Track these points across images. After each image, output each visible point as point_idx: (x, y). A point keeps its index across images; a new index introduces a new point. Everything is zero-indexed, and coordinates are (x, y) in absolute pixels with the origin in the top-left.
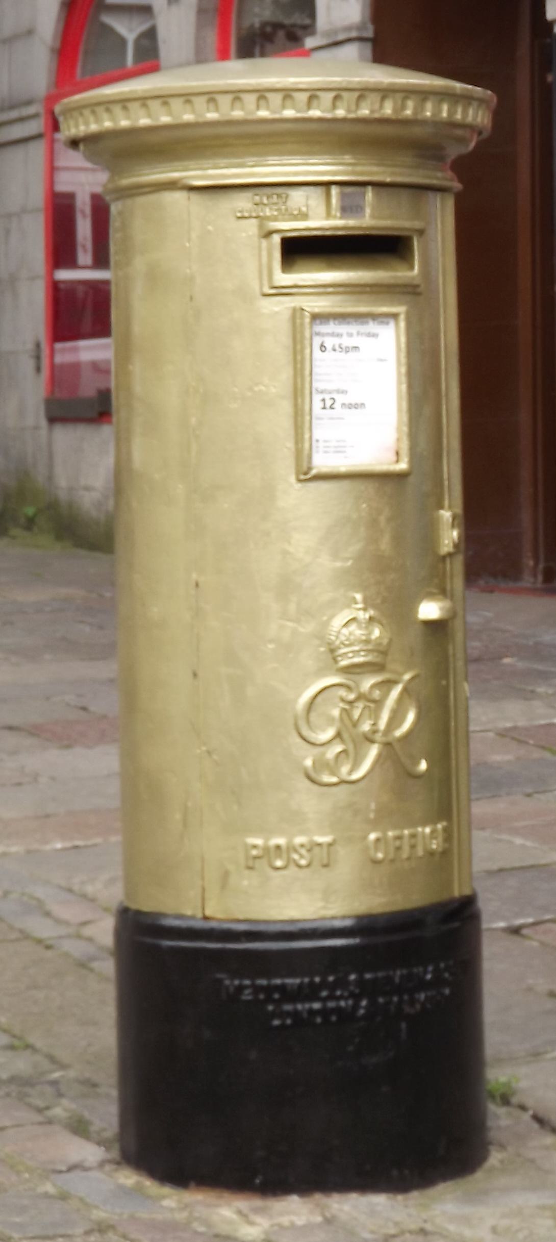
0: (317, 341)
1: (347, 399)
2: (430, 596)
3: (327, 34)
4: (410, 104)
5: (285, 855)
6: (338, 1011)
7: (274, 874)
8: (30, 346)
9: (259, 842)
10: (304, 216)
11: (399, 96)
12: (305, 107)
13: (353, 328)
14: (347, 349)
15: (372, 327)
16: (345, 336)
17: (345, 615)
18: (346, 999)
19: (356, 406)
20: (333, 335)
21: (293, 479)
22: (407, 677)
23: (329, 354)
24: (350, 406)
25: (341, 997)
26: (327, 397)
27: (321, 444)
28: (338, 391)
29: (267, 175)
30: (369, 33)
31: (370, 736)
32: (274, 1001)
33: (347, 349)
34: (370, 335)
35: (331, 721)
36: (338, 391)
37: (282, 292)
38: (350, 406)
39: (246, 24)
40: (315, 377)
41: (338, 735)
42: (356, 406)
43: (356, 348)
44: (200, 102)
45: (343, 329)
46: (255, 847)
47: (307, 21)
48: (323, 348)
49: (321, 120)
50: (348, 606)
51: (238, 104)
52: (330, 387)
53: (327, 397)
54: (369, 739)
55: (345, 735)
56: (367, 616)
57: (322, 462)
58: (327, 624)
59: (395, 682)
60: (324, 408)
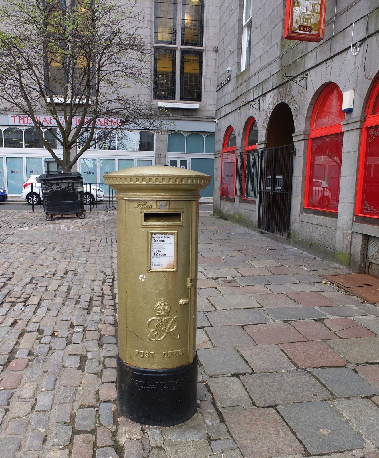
0: (153, 239)
1: (161, 253)
2: (183, 298)
3: (260, 142)
4: (178, 180)
5: (143, 355)
6: (153, 389)
7: (141, 358)
8: (218, 188)
9: (138, 351)
10: (151, 208)
11: (175, 179)
12: (148, 182)
13: (163, 236)
14: (161, 241)
15: (168, 236)
16: (161, 238)
17: (159, 303)
18: (155, 387)
19: (163, 255)
20: (157, 237)
21: (147, 271)
22: (175, 317)
23: (156, 242)
24: (162, 255)
25: (154, 387)
26: (155, 252)
27: (153, 264)
28: (158, 251)
29: (141, 198)
30: (266, 143)
31: (164, 331)
32: (139, 385)
33: (161, 241)
34: (167, 238)
35: (154, 327)
36: (158, 251)
37: (144, 227)
38: (162, 255)
39: (250, 140)
40: (152, 248)
41: (156, 330)
42: (163, 255)
43: (164, 241)
44: (118, 179)
45: (160, 236)
46: (136, 352)
47: (256, 139)
48: (155, 240)
49: (152, 184)
50: (160, 301)
51: (132, 180)
52: (156, 250)
53: (155, 252)
54: (164, 331)
55: (158, 331)
56: (164, 304)
57: (154, 268)
58: (154, 305)
59: (172, 319)
60: (155, 255)
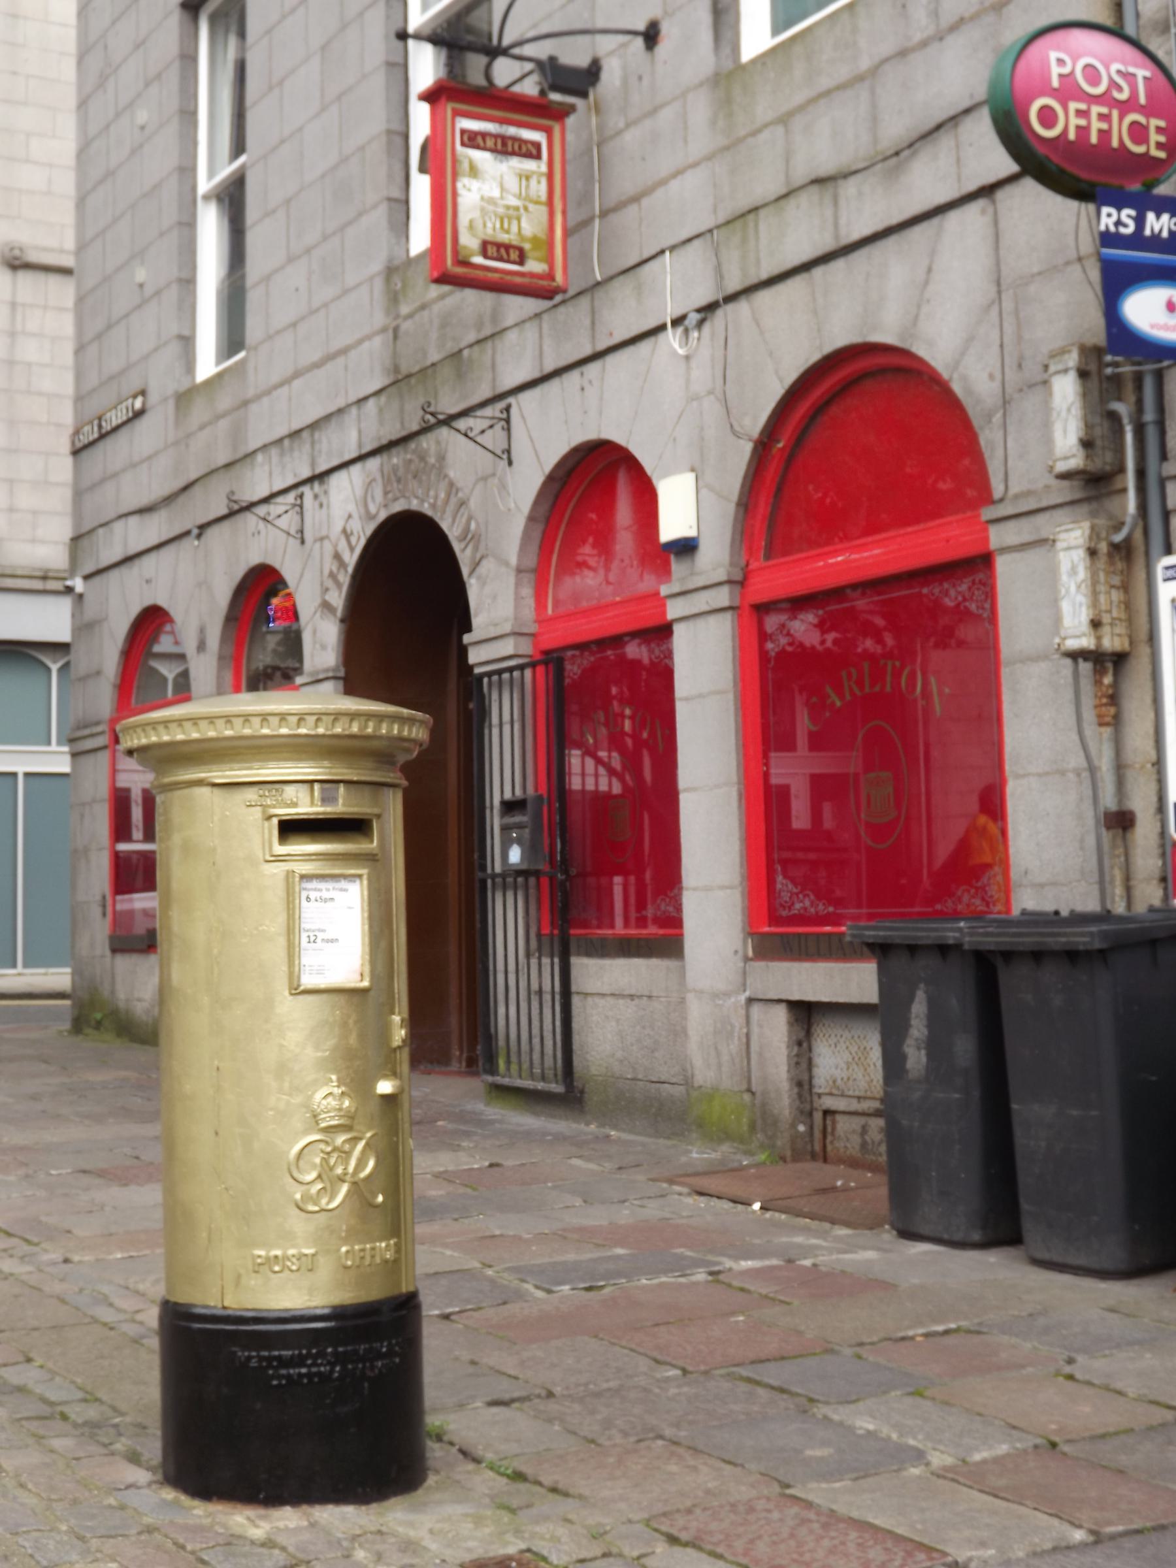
0: (304, 894)
3: (311, 674)
4: (371, 724)
5: (281, 1263)
6: (319, 1374)
8: (98, 898)
9: (262, 1253)
10: (295, 805)
11: (363, 719)
13: (330, 885)
15: (343, 884)
17: (324, 1091)
18: (325, 1366)
19: (332, 941)
20: (315, 890)
21: (286, 993)
22: (369, 1135)
23: (313, 904)
24: (328, 941)
25: (321, 1365)
26: (311, 934)
27: (307, 968)
30: (342, 673)
31: (342, 1177)
33: (326, 901)
34: (342, 890)
35: (314, 1166)
37: (279, 859)
38: (328, 941)
39: (253, 667)
40: (302, 920)
41: (319, 1177)
42: (332, 941)
43: (332, 899)
44: (220, 723)
45: (322, 885)
46: (259, 1257)
47: (297, 665)
49: (307, 736)
50: (327, 1084)
51: (247, 724)
53: (311, 934)
55: (324, 1177)
56: (340, 1091)
57: (308, 980)
58: (311, 1097)
59: (361, 1139)
